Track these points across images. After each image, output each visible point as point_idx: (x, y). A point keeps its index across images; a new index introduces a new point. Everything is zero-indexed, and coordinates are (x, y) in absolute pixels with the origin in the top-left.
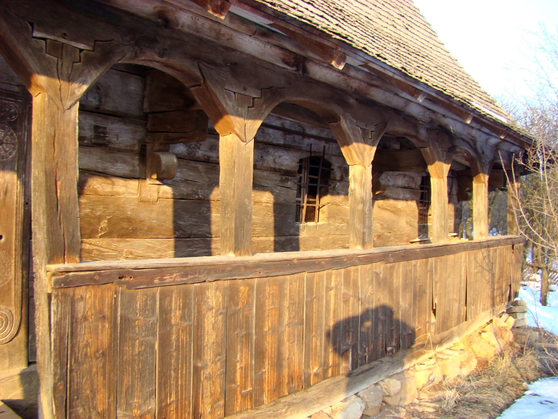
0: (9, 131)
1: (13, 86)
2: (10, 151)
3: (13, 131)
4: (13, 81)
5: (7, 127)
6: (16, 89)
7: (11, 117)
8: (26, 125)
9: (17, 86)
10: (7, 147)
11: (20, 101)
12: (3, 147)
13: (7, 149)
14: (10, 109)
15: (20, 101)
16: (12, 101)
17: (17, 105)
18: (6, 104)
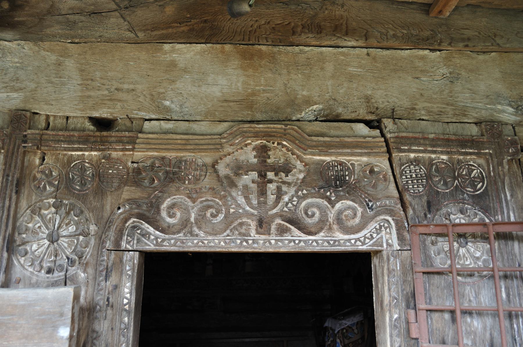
0: (476, 215)
1: (468, 125)
2: (484, 257)
3: (482, 215)
4: (465, 115)
5: (470, 207)
6: (474, 130)
7: (474, 187)
8: (509, 198)
9: (476, 123)
10: (477, 249)
11: (487, 151)
12: (468, 251)
13: (478, 254)
14: (470, 171)
15: (487, 151)
16: (471, 154)
17: (481, 161)
18: (459, 161)
